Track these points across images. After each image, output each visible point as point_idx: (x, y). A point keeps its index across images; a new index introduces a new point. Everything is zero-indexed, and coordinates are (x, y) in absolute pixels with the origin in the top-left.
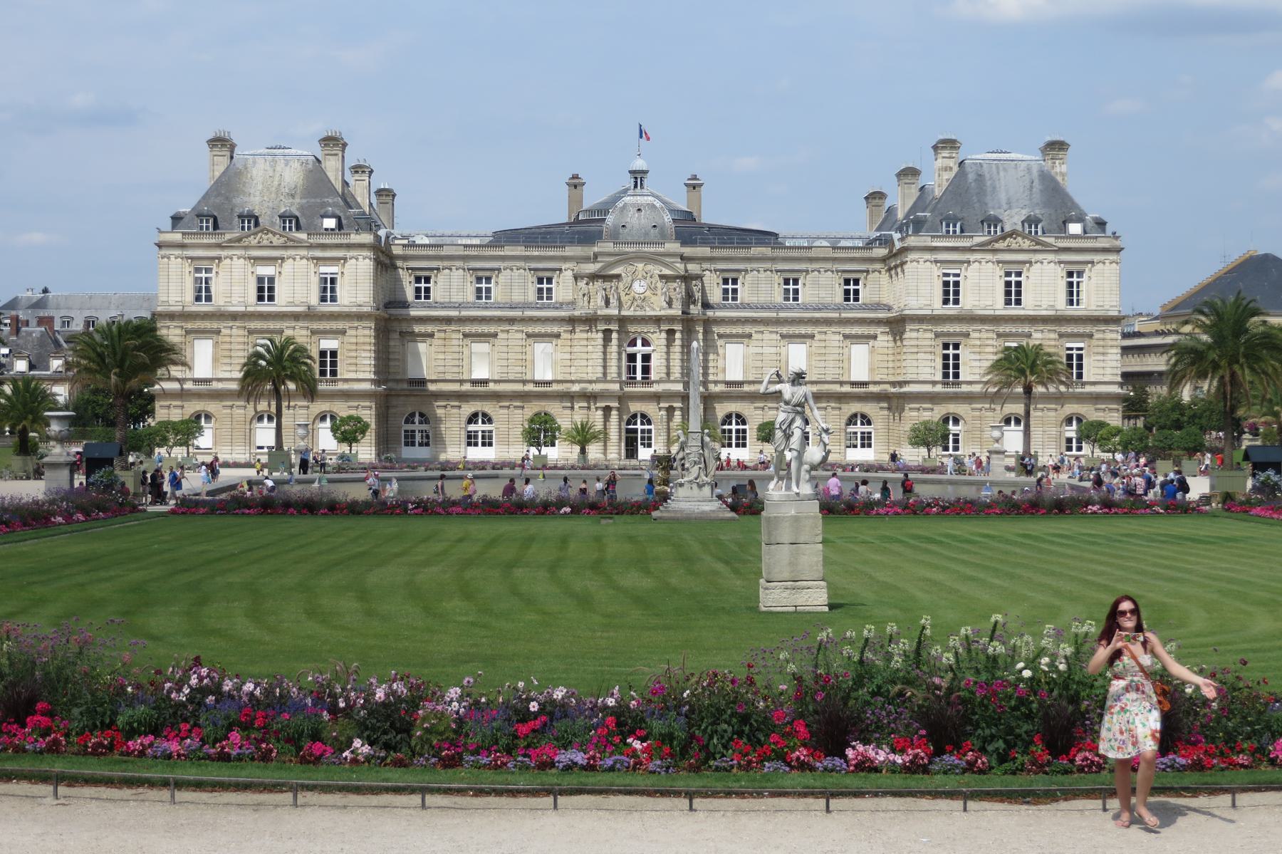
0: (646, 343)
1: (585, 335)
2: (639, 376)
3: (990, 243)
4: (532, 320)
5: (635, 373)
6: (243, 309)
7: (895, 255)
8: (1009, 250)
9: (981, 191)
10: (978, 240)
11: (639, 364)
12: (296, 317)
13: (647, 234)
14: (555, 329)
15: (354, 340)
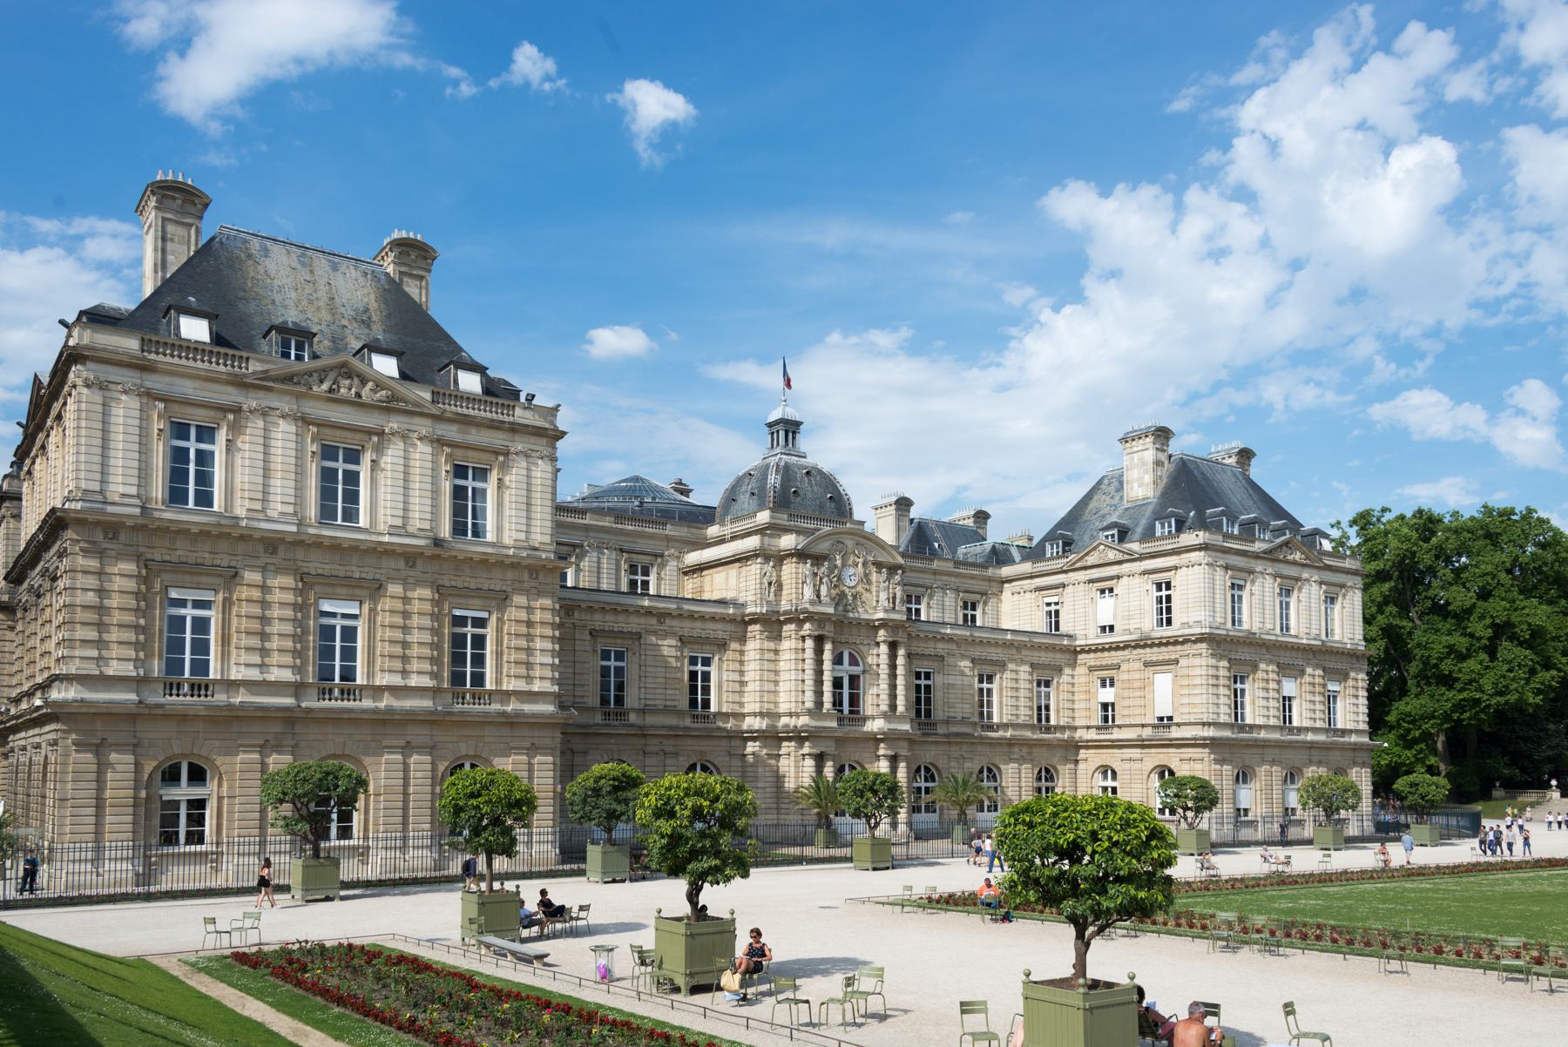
0: (854, 662)
1: (772, 645)
2: (846, 707)
3: (1270, 551)
4: (691, 616)
5: (841, 704)
6: (294, 529)
7: (1085, 568)
8: (1287, 562)
9: (1217, 493)
10: (1258, 546)
11: (846, 691)
12: (410, 557)
13: (821, 507)
14: (719, 631)
15: (523, 615)
